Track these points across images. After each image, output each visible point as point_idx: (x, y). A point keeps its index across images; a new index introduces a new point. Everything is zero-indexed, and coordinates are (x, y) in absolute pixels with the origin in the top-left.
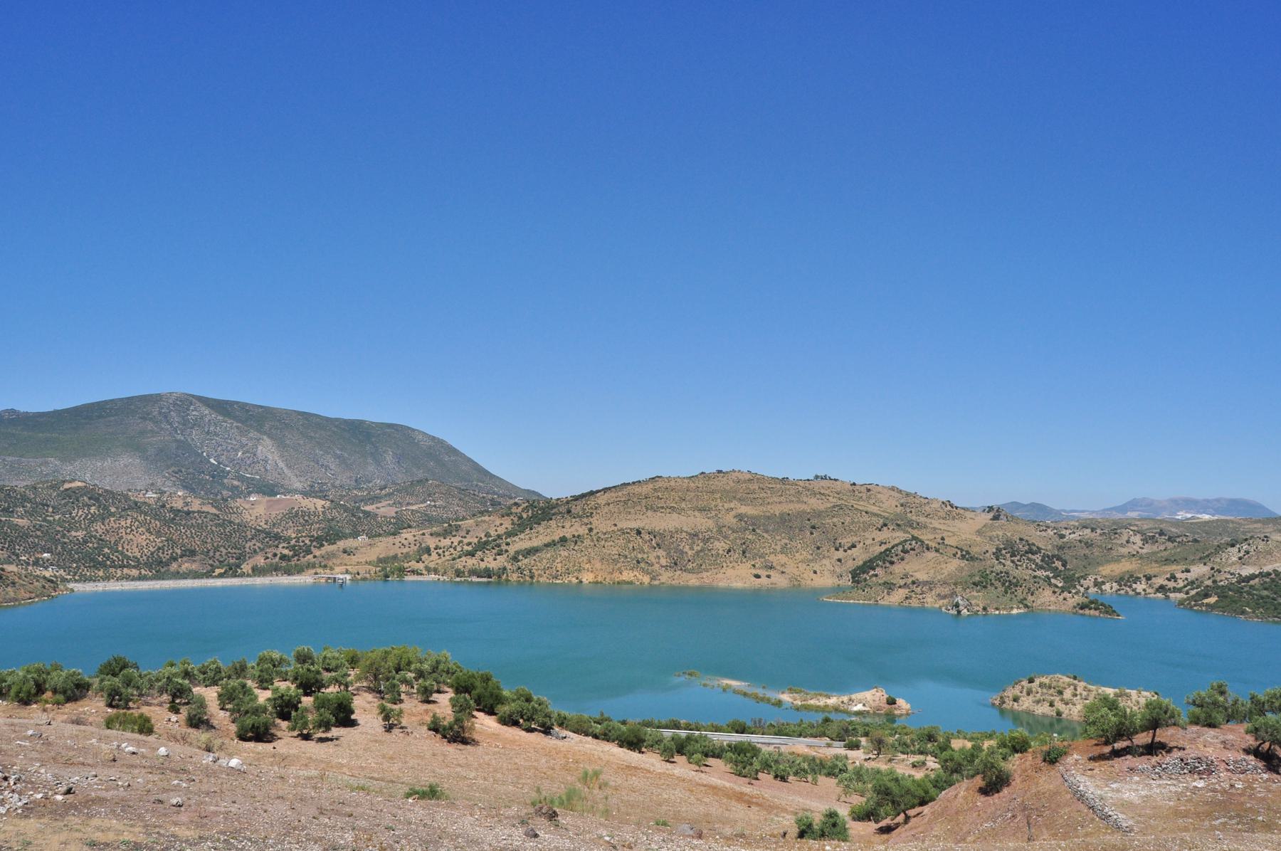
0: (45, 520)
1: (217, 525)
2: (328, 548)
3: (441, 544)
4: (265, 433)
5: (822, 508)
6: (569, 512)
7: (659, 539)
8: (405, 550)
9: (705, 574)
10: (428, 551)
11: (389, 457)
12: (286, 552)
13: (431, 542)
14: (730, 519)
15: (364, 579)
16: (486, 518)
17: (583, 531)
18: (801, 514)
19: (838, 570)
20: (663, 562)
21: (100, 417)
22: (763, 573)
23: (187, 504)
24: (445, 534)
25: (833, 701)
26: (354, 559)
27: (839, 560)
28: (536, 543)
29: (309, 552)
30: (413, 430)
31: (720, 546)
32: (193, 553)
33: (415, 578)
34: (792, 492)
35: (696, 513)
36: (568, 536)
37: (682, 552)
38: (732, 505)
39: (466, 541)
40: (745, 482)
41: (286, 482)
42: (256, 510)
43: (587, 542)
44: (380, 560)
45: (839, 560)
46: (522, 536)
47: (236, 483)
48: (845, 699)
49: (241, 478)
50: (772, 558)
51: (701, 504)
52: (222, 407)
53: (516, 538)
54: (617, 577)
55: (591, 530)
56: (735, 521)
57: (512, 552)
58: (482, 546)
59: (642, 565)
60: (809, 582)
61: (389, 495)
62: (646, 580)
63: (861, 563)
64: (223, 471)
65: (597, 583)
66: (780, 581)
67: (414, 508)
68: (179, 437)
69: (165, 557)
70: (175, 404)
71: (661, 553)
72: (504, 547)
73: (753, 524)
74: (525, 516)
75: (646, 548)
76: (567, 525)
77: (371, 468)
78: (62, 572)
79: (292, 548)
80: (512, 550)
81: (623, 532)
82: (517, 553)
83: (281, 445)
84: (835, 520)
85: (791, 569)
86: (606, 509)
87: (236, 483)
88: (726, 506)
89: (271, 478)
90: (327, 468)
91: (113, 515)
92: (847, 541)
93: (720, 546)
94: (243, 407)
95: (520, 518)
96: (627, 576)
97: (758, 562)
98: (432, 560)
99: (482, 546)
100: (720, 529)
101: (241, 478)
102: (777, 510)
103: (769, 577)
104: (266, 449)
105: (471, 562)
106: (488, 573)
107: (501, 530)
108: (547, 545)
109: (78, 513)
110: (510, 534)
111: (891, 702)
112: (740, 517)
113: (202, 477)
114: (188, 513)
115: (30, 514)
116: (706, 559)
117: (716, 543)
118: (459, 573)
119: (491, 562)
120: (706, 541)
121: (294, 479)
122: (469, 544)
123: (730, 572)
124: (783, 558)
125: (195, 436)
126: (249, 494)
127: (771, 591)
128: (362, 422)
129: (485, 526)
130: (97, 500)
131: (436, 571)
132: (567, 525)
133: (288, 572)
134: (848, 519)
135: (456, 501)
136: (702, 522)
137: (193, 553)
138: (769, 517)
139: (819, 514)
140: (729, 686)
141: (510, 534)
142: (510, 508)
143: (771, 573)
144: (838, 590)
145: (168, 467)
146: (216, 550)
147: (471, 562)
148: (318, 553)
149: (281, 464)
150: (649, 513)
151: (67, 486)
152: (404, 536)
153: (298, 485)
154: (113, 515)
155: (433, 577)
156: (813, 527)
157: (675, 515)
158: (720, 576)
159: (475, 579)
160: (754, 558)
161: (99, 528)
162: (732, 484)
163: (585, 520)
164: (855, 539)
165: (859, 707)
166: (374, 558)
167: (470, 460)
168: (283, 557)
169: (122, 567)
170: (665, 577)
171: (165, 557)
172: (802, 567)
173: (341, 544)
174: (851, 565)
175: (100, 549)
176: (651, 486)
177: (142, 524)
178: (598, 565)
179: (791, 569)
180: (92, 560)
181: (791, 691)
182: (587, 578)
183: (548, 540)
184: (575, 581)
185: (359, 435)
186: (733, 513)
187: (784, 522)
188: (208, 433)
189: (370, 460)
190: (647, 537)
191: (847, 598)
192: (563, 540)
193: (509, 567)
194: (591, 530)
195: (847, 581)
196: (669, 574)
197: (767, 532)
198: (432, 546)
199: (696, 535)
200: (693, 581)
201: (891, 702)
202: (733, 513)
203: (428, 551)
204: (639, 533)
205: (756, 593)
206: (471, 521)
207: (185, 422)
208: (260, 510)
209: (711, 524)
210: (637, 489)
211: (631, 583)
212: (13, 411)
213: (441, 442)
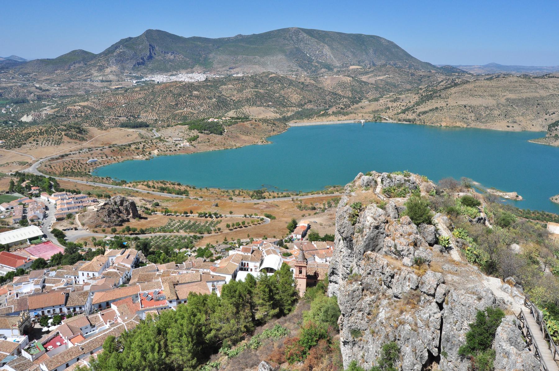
0: (267, 90)
1: (317, 90)
2: (356, 106)
3: (393, 106)
4: (326, 43)
5: (545, 95)
6: (440, 96)
7: (473, 109)
8: (381, 108)
9: (489, 124)
10: (389, 108)
11: (371, 51)
12: (342, 106)
13: (390, 104)
14: (503, 101)
15: (369, 122)
16: (409, 95)
17: (444, 104)
18: (534, 98)
19: (544, 124)
20: (473, 118)
21: (270, 38)
22: (510, 125)
23: (305, 80)
24: (395, 101)
25: (501, 194)
26: (364, 111)
27: (546, 119)
28: (427, 109)
29: (350, 107)
30: (381, 38)
31: (496, 112)
32: (311, 101)
33: (385, 121)
34: (534, 87)
35: (490, 98)
36: (439, 107)
37: (481, 115)
38: (505, 94)
39: (402, 104)
40: (514, 82)
41: (334, 63)
42: (328, 81)
43: (445, 110)
44: (373, 112)
45: (546, 119)
46: (422, 106)
47: (316, 64)
48: (504, 194)
49: (318, 62)
50: (517, 118)
51: (492, 93)
52: (310, 32)
53: (420, 107)
54: (455, 124)
55: (447, 104)
56: (505, 101)
57: (418, 113)
58: (408, 109)
59: (465, 120)
60: (529, 130)
61: (372, 71)
62: (465, 126)
63: (554, 121)
64: (312, 59)
65: (447, 126)
66: (517, 128)
67: (381, 78)
68: (297, 46)
69: (303, 103)
70: (294, 33)
71: (473, 115)
72: (415, 110)
73: (513, 103)
74: (424, 95)
75: (467, 113)
76: (439, 102)
77: (364, 56)
78: (275, 109)
79: (344, 105)
80: (418, 111)
81: (459, 106)
82: (420, 113)
83: (332, 49)
84: (549, 101)
85: (524, 124)
86: (454, 95)
87: (316, 64)
88: (503, 94)
89: (328, 62)
90: (348, 57)
91: (285, 87)
92: (551, 111)
93: (496, 112)
94: (318, 31)
95: (422, 95)
96: (458, 124)
97: (511, 119)
98: (391, 113)
99: (408, 109)
100: (498, 105)
101: (318, 62)
102: (524, 96)
103: (513, 127)
104: (327, 50)
105: (403, 116)
106: (409, 121)
107: (415, 100)
108: (431, 110)
109: (275, 86)
110: (418, 104)
111: (517, 196)
112: (507, 100)
113: (305, 63)
114: (307, 85)
115: (262, 87)
116: (490, 118)
117: (495, 111)
118: (399, 120)
119: (411, 116)
120: (491, 110)
121: (336, 62)
122: (403, 106)
123: (498, 124)
124: (521, 118)
125: (302, 45)
126: (321, 68)
127: (512, 133)
128: (361, 35)
129: (409, 98)
130: (280, 81)
131: (392, 119)
132: (439, 102)
133: (344, 114)
134: (555, 101)
135: (397, 75)
136: (491, 102)
137: (311, 101)
138: (520, 99)
139: (542, 98)
140: (474, 185)
141: (418, 104)
142: (418, 91)
143: (515, 125)
144: (541, 135)
145: (294, 58)
146: (318, 100)
147: (403, 116)
148: (352, 107)
149: (332, 56)
150: (471, 97)
151: (271, 76)
152: (381, 101)
153: (338, 65)
154: (285, 87)
155: (391, 121)
156: (538, 104)
157: (481, 99)
158: (494, 125)
159: (405, 123)
160: (509, 118)
161: (282, 92)
162: (508, 83)
163: (446, 100)
164: (556, 110)
165: (507, 197)
166: (370, 110)
167: (403, 50)
168: (342, 108)
169: (291, 107)
170: (473, 125)
171: (303, 103)
172: (529, 122)
173: (360, 104)
174: (550, 122)
175: (284, 100)
176: (473, 85)
177: (295, 91)
178: (448, 119)
179: (524, 124)
180: (283, 104)
181: (492, 188)
182: (444, 124)
183: (431, 108)
184: (439, 125)
185: (360, 42)
186: (505, 98)
187: (526, 102)
188: (306, 44)
189: (364, 53)
190: (468, 108)
191: (538, 142)
192: (437, 108)
193: (417, 118)
194: (447, 104)
195: (545, 129)
196: (474, 124)
197: (517, 106)
198: (390, 106)
199: (488, 108)
200: (482, 126)
201: (517, 196)
202: (505, 98)
203: (389, 108)
204: (465, 106)
205: (507, 133)
206: (404, 96)
207: (298, 40)
208: (329, 82)
209: (494, 102)
210: (467, 86)
211: (459, 127)
212: (240, 35)
213: (392, 43)
